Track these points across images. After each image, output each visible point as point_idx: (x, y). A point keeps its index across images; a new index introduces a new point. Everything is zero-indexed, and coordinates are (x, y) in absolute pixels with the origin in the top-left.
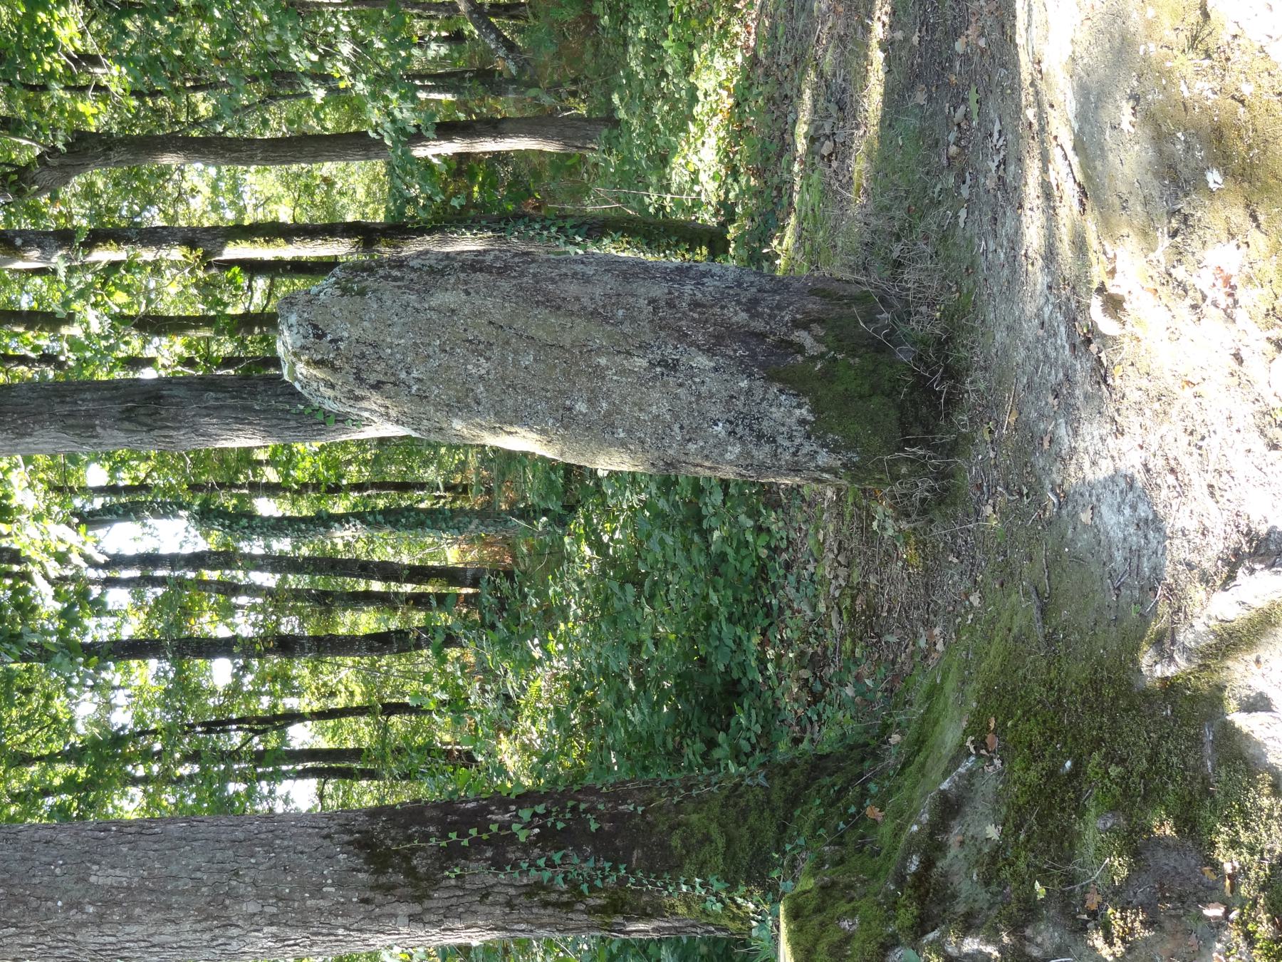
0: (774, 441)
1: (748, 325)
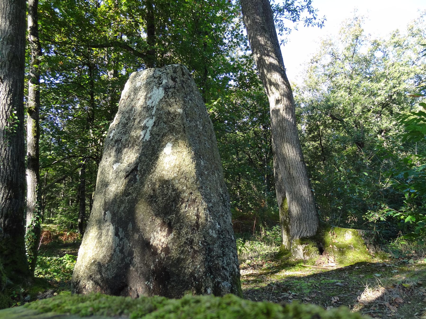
0: (224, 255)
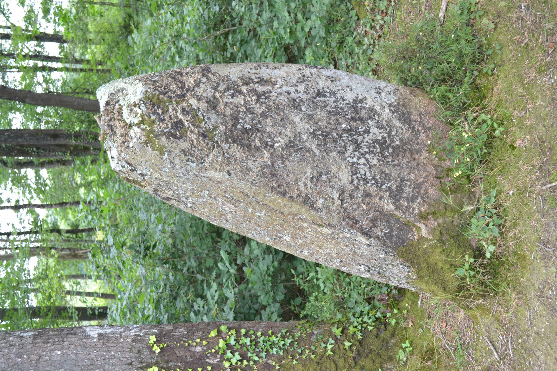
1: (393, 211)
